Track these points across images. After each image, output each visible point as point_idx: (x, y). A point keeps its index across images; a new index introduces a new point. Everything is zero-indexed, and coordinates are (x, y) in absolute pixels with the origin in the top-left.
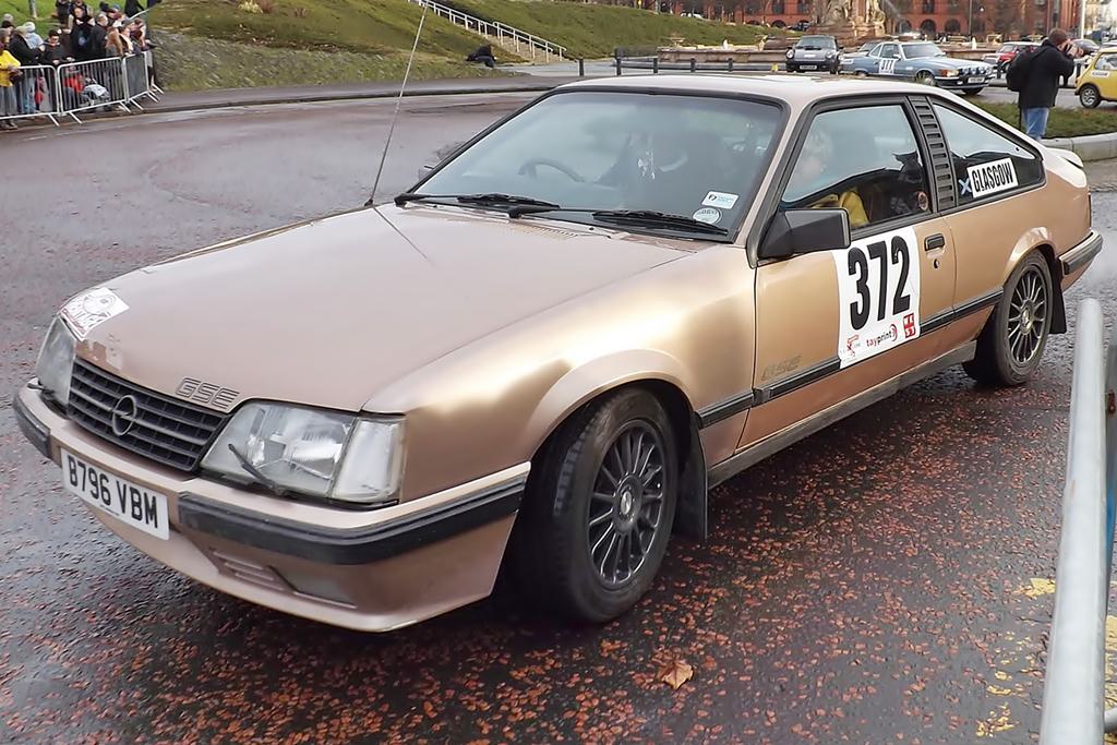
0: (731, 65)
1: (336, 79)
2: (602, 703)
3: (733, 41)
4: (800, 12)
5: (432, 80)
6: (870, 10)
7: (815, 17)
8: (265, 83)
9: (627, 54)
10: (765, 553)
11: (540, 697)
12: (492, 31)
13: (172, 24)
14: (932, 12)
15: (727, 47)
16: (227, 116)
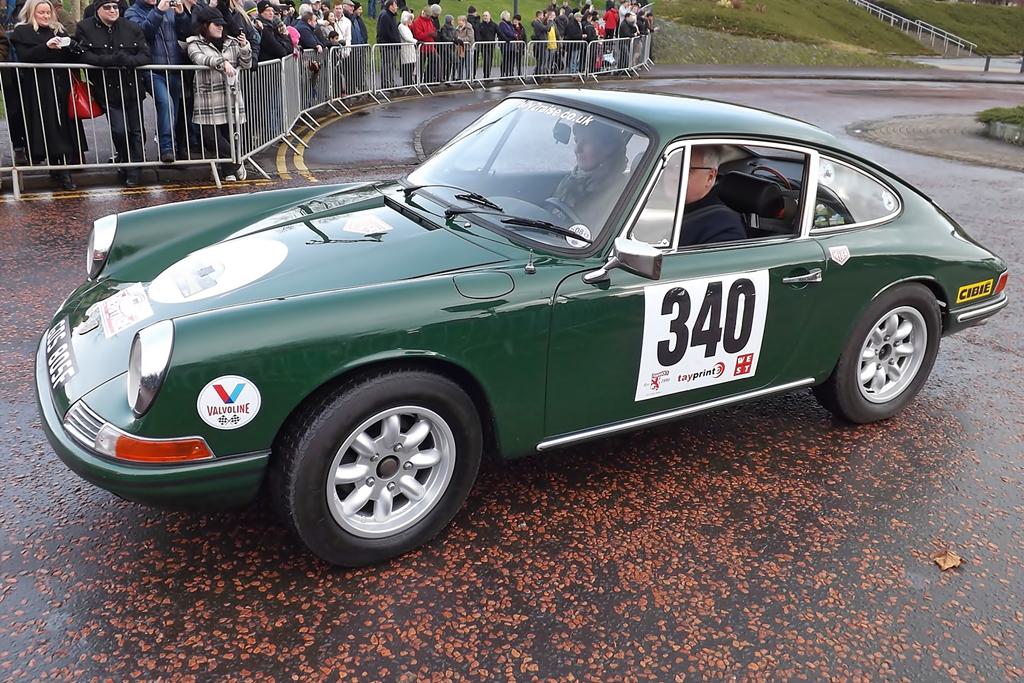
1: (777, 64)
2: (881, 561)
5: (854, 67)
11: (837, 541)
12: (913, 28)
13: (669, 14)
16: (695, 85)
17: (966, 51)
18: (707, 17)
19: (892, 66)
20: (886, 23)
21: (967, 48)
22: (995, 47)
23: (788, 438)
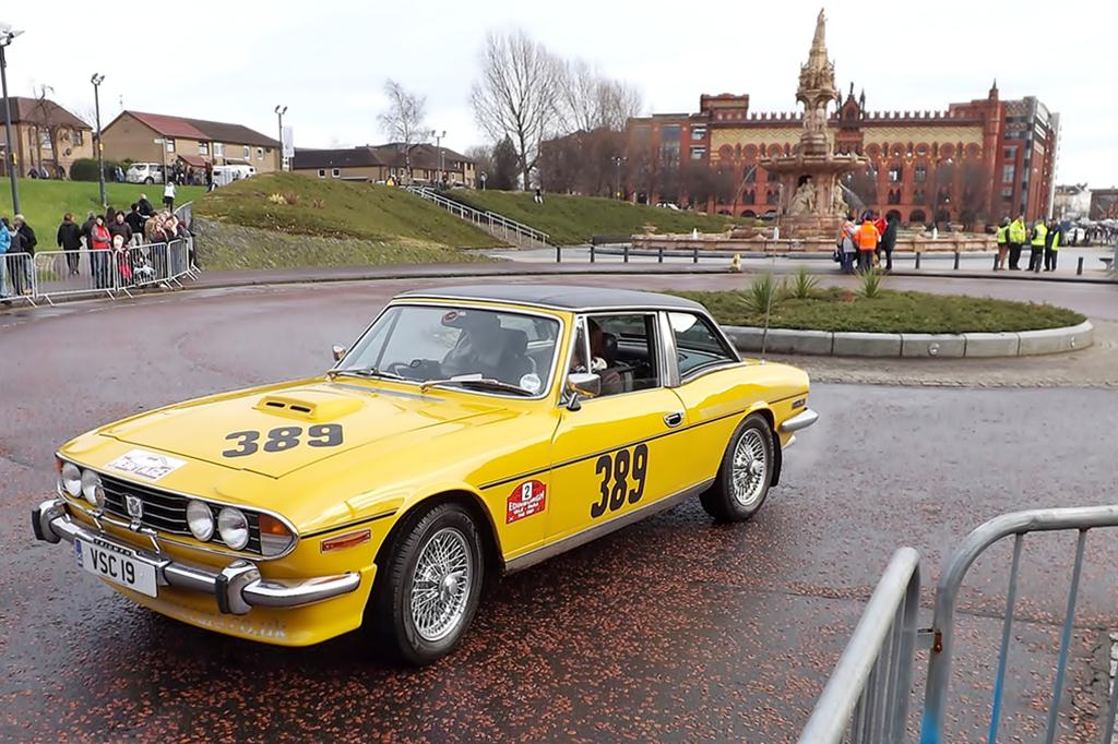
0: (696, 253)
3: (702, 229)
4: (769, 202)
5: (426, 265)
6: (835, 202)
7: (780, 209)
8: (285, 265)
9: (603, 241)
10: (644, 733)
12: (484, 220)
13: (212, 214)
14: (898, 203)
15: (695, 235)
17: (540, 242)
18: (257, 215)
19: (466, 262)
20: (457, 215)
21: (540, 239)
22: (567, 237)
23: (357, 725)
